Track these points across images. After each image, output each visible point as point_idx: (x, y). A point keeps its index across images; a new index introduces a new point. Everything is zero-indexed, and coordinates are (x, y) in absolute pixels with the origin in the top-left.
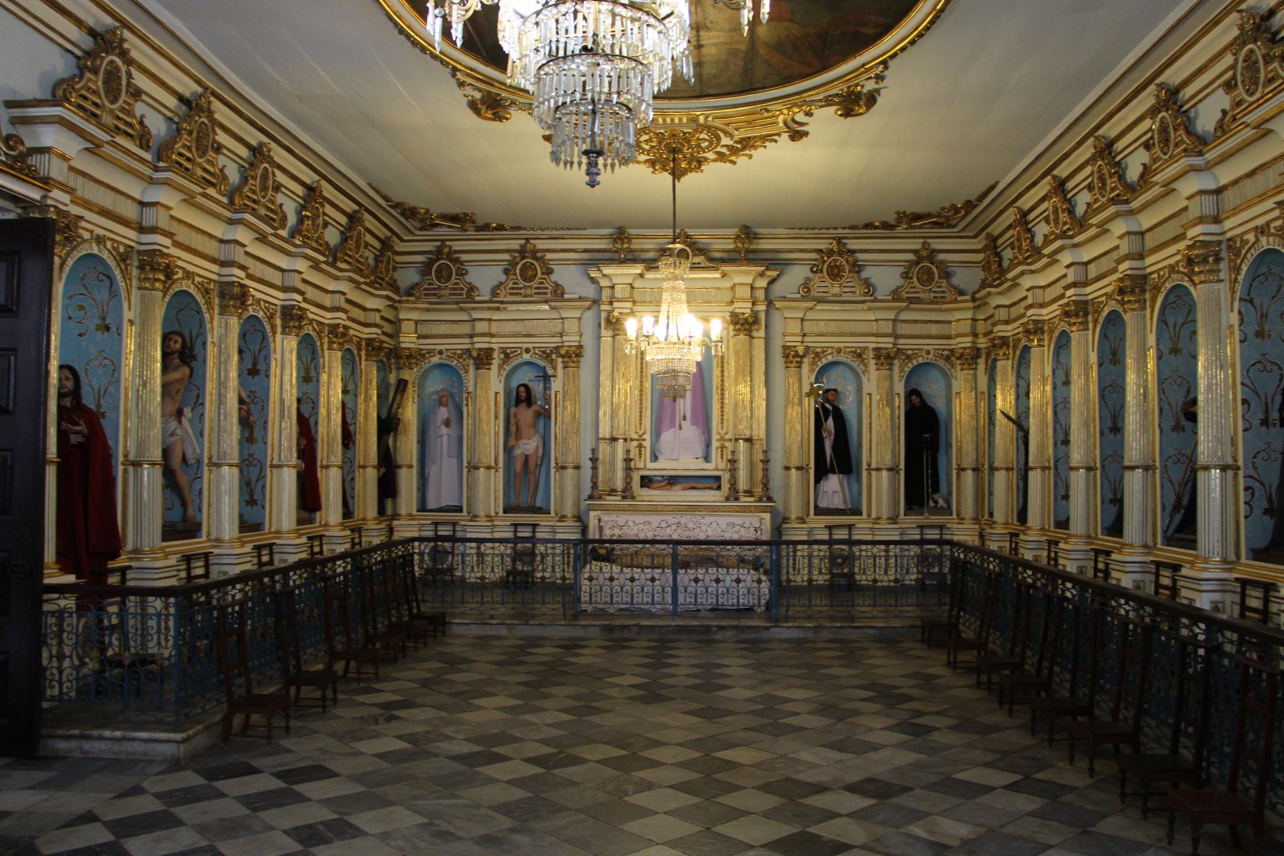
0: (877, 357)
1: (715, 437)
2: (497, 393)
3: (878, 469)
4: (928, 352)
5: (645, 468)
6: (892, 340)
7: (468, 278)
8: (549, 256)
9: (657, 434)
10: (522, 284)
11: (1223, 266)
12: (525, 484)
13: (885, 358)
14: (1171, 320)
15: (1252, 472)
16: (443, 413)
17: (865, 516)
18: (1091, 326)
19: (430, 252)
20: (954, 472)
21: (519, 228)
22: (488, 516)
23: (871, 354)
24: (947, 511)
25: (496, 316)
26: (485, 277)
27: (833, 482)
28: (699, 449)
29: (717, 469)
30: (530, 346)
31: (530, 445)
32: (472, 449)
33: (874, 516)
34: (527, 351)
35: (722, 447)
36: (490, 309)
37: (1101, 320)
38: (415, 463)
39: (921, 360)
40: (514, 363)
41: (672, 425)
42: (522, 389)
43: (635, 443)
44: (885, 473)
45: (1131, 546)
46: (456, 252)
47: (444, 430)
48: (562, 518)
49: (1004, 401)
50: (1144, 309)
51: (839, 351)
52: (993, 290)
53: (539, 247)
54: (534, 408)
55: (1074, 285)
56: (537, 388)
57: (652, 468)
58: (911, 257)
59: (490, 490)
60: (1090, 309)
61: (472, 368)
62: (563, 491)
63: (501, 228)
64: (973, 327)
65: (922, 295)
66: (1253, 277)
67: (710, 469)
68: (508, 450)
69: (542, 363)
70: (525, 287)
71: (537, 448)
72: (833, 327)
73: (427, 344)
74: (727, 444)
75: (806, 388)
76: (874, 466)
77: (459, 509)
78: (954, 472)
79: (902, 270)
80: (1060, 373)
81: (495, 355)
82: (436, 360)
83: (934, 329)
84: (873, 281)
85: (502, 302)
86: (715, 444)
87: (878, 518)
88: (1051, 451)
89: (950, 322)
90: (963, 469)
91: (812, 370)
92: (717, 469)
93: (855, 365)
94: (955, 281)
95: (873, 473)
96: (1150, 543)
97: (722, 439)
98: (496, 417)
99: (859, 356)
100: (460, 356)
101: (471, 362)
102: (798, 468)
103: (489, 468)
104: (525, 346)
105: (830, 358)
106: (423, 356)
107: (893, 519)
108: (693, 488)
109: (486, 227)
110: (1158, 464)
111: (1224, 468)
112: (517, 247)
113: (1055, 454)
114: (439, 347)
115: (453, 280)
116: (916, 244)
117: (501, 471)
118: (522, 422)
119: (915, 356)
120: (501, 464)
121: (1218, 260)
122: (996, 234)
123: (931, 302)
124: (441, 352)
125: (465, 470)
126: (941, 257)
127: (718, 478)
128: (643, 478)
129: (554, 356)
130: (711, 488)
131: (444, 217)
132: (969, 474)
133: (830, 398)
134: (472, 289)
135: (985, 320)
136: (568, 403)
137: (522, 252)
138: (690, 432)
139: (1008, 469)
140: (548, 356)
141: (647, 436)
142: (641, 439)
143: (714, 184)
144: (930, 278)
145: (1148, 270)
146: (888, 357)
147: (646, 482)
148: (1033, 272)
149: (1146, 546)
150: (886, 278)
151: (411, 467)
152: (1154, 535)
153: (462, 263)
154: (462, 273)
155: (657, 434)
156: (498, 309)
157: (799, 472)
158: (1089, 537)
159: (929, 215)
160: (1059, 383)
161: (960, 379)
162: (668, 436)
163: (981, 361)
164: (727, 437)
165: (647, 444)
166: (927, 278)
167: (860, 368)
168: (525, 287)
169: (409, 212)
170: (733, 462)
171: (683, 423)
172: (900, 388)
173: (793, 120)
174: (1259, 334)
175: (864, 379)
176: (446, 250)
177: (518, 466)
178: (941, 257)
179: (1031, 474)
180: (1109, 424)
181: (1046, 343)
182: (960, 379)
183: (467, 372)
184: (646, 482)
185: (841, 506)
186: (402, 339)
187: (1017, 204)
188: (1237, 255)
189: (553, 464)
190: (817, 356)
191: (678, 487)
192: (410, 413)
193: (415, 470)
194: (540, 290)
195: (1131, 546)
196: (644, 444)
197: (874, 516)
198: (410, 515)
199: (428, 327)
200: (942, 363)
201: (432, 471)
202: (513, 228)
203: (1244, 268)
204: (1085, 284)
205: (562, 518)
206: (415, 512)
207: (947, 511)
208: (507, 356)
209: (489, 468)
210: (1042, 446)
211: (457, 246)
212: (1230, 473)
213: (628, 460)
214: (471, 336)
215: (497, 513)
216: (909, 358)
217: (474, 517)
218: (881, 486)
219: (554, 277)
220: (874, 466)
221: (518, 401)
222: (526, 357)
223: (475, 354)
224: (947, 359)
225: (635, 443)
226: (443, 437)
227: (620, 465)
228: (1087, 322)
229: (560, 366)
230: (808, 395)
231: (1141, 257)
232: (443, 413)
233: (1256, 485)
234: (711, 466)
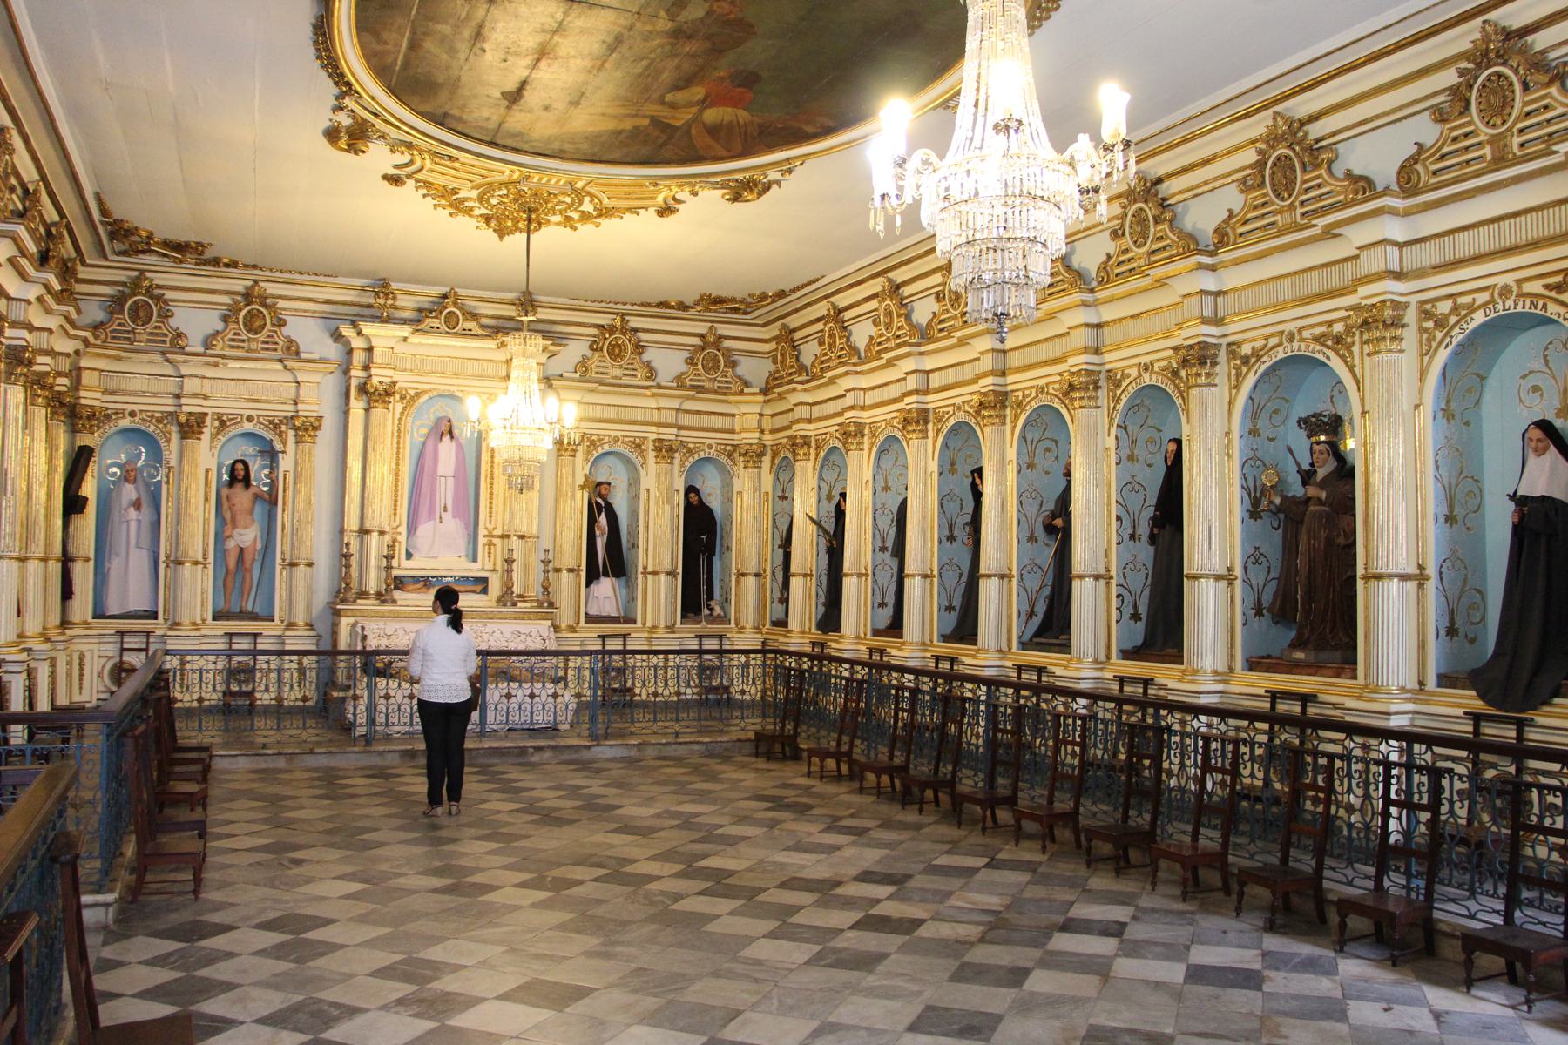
0: (658, 449)
1: (482, 532)
2: (207, 470)
3: (655, 573)
4: (710, 447)
6: (674, 431)
7: (174, 322)
8: (281, 304)
9: (412, 529)
10: (245, 335)
11: (1102, 393)
12: (243, 584)
13: (665, 450)
14: (1029, 438)
15: (1122, 581)
16: (129, 492)
17: (639, 624)
18: (931, 434)
19: (124, 284)
20: (734, 578)
21: (254, 267)
22: (194, 624)
23: (651, 446)
24: (724, 619)
26: (195, 321)
27: (605, 586)
28: (462, 544)
30: (254, 413)
31: (247, 535)
32: (177, 538)
33: (649, 624)
34: (250, 419)
35: (490, 544)
36: (207, 364)
37: (945, 430)
38: (92, 555)
39: (702, 455)
42: (240, 466)
44: (663, 577)
45: (987, 651)
46: (158, 287)
47: (133, 513)
48: (291, 626)
49: (805, 502)
50: (1004, 424)
51: (616, 440)
52: (800, 387)
53: (269, 292)
54: (252, 490)
55: (917, 392)
58: (696, 341)
59: (197, 589)
60: (931, 417)
61: (175, 437)
62: (301, 594)
63: (233, 264)
64: (759, 422)
65: (706, 384)
66: (1132, 407)
67: (476, 570)
68: (220, 538)
69: (268, 435)
71: (255, 540)
72: (611, 413)
73: (113, 402)
74: (496, 541)
75: (580, 480)
76: (650, 569)
77: (154, 615)
78: (734, 578)
79: (686, 355)
80: (880, 478)
81: (208, 420)
82: (125, 423)
83: (718, 422)
84: (653, 364)
85: (223, 357)
86: (482, 541)
87: (654, 627)
88: (868, 557)
89: (733, 415)
90: (743, 575)
93: (633, 456)
94: (740, 371)
95: (650, 577)
96: (1005, 648)
97: (490, 535)
98: (206, 499)
99: (639, 446)
100: (159, 421)
101: (175, 428)
102: (570, 570)
103: (196, 563)
105: (606, 448)
106: (108, 417)
107: (671, 628)
109: (216, 262)
110: (1014, 572)
111: (1097, 578)
112: (241, 289)
113: (874, 560)
114: (130, 408)
115: (153, 322)
116: (702, 328)
119: (697, 450)
121: (1097, 388)
122: (792, 326)
123: (716, 393)
124: (133, 414)
125: (162, 566)
126: (727, 344)
127: (485, 581)
129: (283, 428)
131: (166, 244)
132: (751, 580)
134: (179, 335)
135: (772, 416)
136: (301, 486)
137: (248, 296)
138: (452, 526)
139: (805, 575)
140: (276, 427)
143: (562, 248)
144: (716, 367)
145: (1009, 388)
146: (670, 449)
147: (400, 583)
148: (857, 373)
149: (1000, 651)
150: (669, 363)
151: (87, 560)
152: (1009, 640)
153: (166, 302)
154: (166, 315)
155: (412, 529)
156: (216, 365)
157: (572, 575)
158: (924, 644)
159: (734, 300)
160: (879, 489)
161: (743, 480)
162: (424, 529)
163: (767, 460)
164: (496, 533)
165: (402, 538)
166: (712, 366)
167: (638, 461)
169: (120, 231)
170: (510, 561)
172: (680, 485)
173: (674, 198)
174: (1131, 458)
175: (642, 472)
176: (147, 283)
177: (232, 563)
178: (727, 344)
179: (907, 582)
180: (947, 533)
181: (866, 446)
182: (743, 480)
183: (168, 441)
185: (614, 614)
186: (82, 394)
187: (832, 299)
188: (1118, 385)
189: (279, 560)
192: (89, 489)
193: (92, 563)
194: (268, 346)
195: (987, 651)
196: (399, 538)
197: (649, 624)
198: (86, 623)
199: (131, 382)
200: (723, 459)
201: (114, 566)
202: (246, 266)
203: (1124, 399)
204: (927, 392)
205: (291, 626)
206: (90, 620)
207: (724, 619)
208: (223, 423)
209: (196, 563)
210: (858, 554)
211: (159, 279)
212: (1102, 582)
214: (178, 396)
215: (204, 621)
216: (690, 451)
217: (175, 625)
218: (659, 594)
219: (286, 331)
220: (650, 569)
222: (248, 427)
223: (183, 419)
224: (730, 455)
226: (131, 524)
228: (927, 431)
230: (582, 487)
231: (1003, 374)
232: (129, 492)
233: (1125, 593)
234: (477, 565)
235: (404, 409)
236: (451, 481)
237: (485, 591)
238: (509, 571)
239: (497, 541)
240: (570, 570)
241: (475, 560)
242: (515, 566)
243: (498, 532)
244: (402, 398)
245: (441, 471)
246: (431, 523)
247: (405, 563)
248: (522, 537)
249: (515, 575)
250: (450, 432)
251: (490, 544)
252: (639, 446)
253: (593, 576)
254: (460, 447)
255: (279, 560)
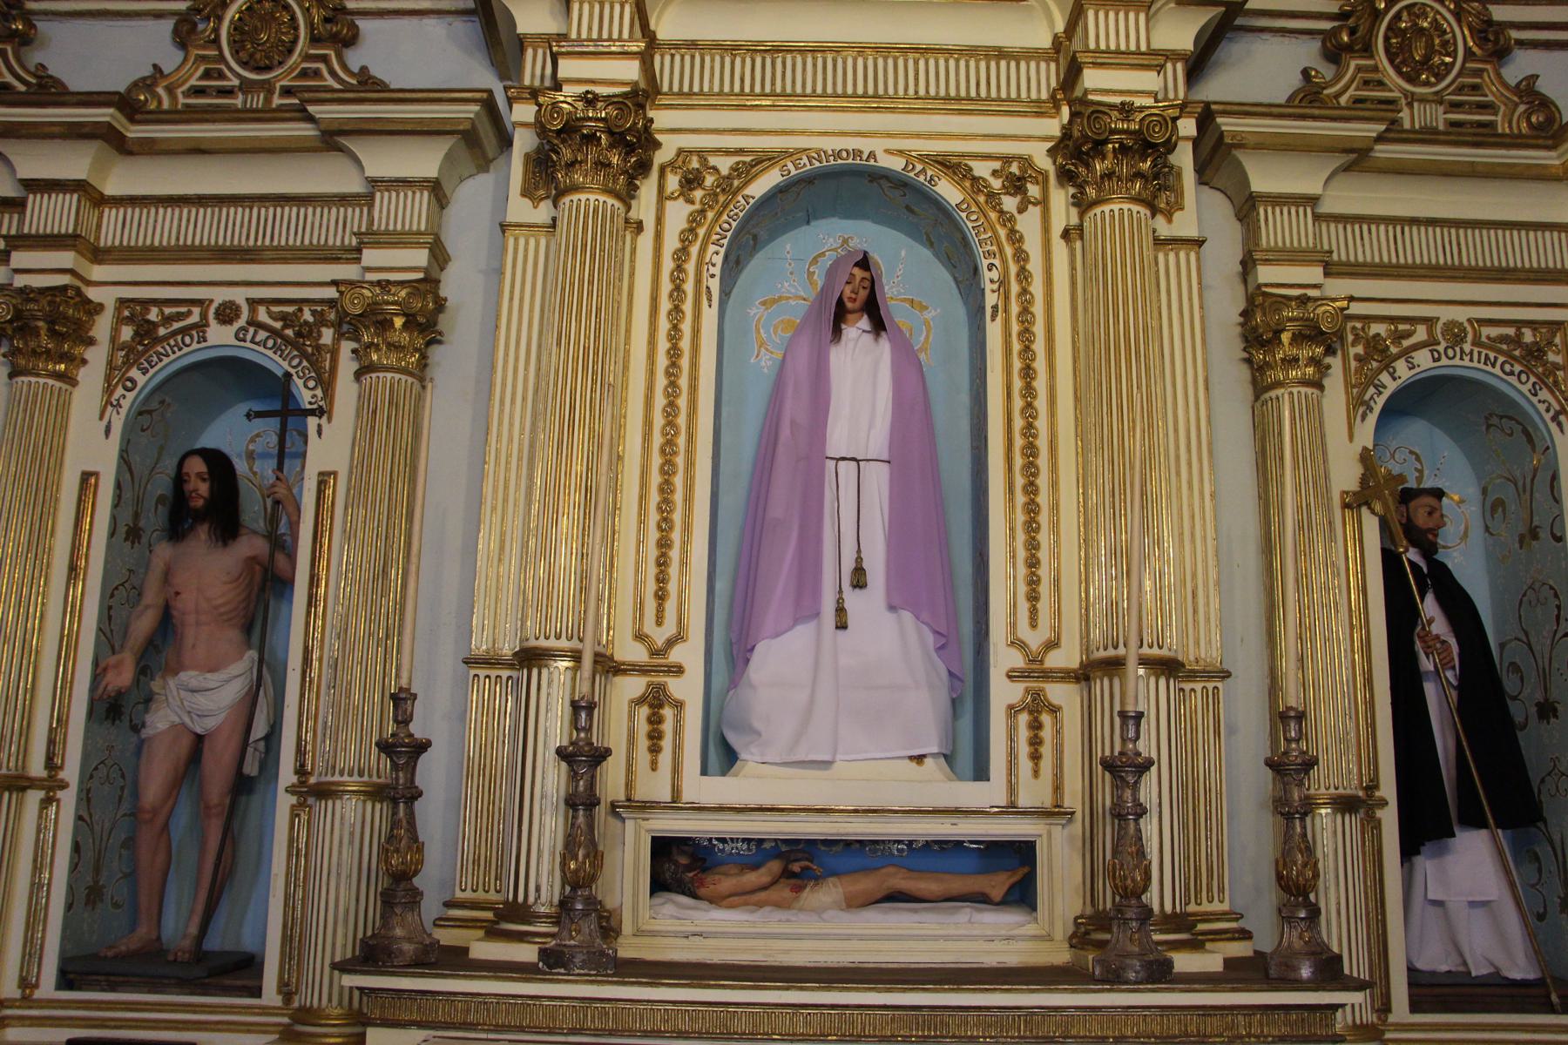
1: (1003, 658)
5: (674, 804)
9: (734, 649)
10: (235, 73)
25: (120, 180)
27: (1472, 863)
28: (923, 711)
29: (1011, 809)
30: (239, 295)
31: (204, 695)
34: (227, 313)
35: (1037, 706)
40: (171, 360)
41: (805, 609)
42: (197, 466)
43: (633, 686)
51: (1455, 334)
56: (254, 475)
57: (716, 804)
67: (977, 808)
68: (112, 710)
69: (277, 363)
70: (247, 87)
72: (1423, 247)
74: (1058, 693)
75: (1345, 475)
81: (102, 328)
84: (1543, 86)
86: (1003, 693)
91: (1357, 405)
92: (1011, 809)
97: (1034, 671)
99: (1535, 354)
102: (1345, 805)
104: (219, 295)
108: (896, 897)
117: (68, 799)
118: (187, 603)
120: (71, 772)
127: (1021, 854)
128: (663, 847)
129: (327, 336)
130: (980, 899)
133: (1421, 519)
138: (887, 636)
140: (307, 332)
141: (690, 654)
142: (660, 665)
147: (681, 866)
155: (734, 649)
157: (1353, 822)
162: (781, 658)
164: (1055, 660)
165: (688, 689)
168: (247, 87)
170: (1125, 769)
171: (852, 599)
184: (681, 866)
190: (1378, 354)
191: (828, 893)
196: (675, 686)
208: (145, 332)
213: (583, 758)
221: (180, 518)
222: (220, 336)
225: (633, 686)
227: (551, 779)
229: (347, 366)
230: (1355, 502)
234: (992, 793)
235: (695, 220)
236: (878, 479)
237: (1023, 895)
238: (1127, 814)
239: (1062, 694)
240: (1345, 805)
241: (981, 773)
242: (1150, 789)
243: (1067, 657)
244: (691, 182)
245: (838, 440)
246: (801, 636)
247: (699, 788)
248: (1167, 667)
249: (1149, 827)
250: (872, 309)
251: (1037, 706)
252: (1535, 354)
253: (1424, 828)
254: (907, 363)
255: (287, 774)
